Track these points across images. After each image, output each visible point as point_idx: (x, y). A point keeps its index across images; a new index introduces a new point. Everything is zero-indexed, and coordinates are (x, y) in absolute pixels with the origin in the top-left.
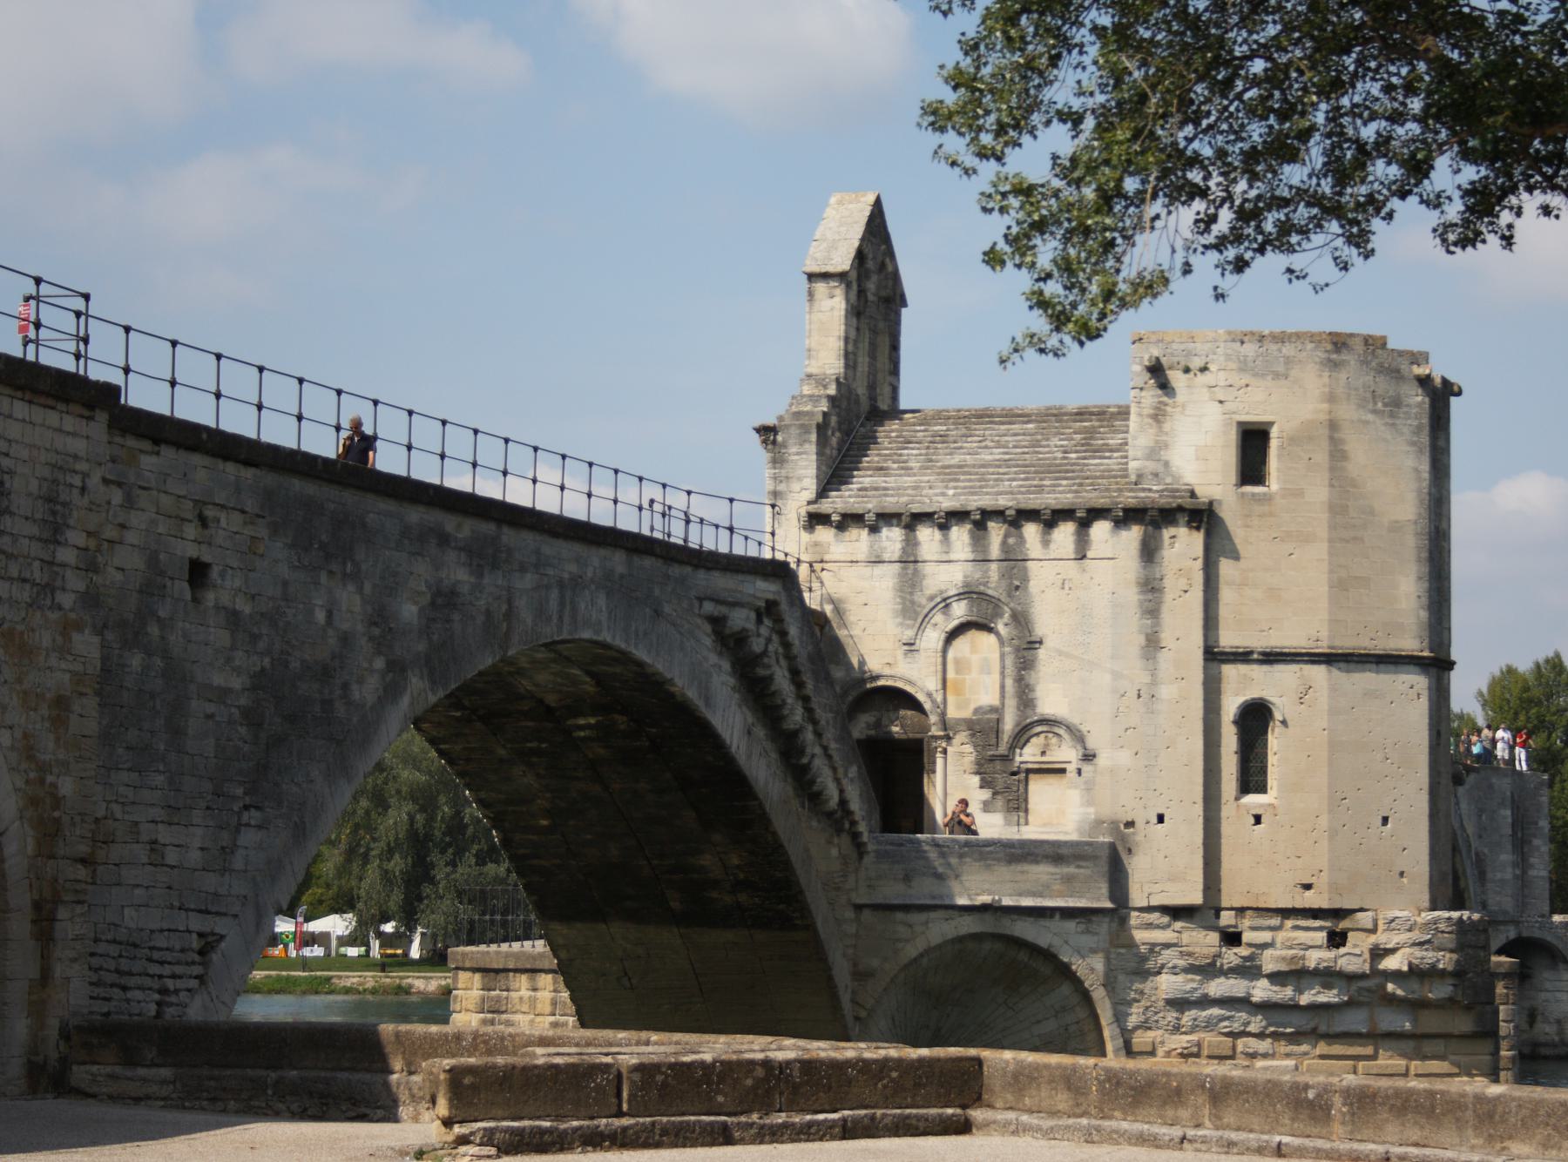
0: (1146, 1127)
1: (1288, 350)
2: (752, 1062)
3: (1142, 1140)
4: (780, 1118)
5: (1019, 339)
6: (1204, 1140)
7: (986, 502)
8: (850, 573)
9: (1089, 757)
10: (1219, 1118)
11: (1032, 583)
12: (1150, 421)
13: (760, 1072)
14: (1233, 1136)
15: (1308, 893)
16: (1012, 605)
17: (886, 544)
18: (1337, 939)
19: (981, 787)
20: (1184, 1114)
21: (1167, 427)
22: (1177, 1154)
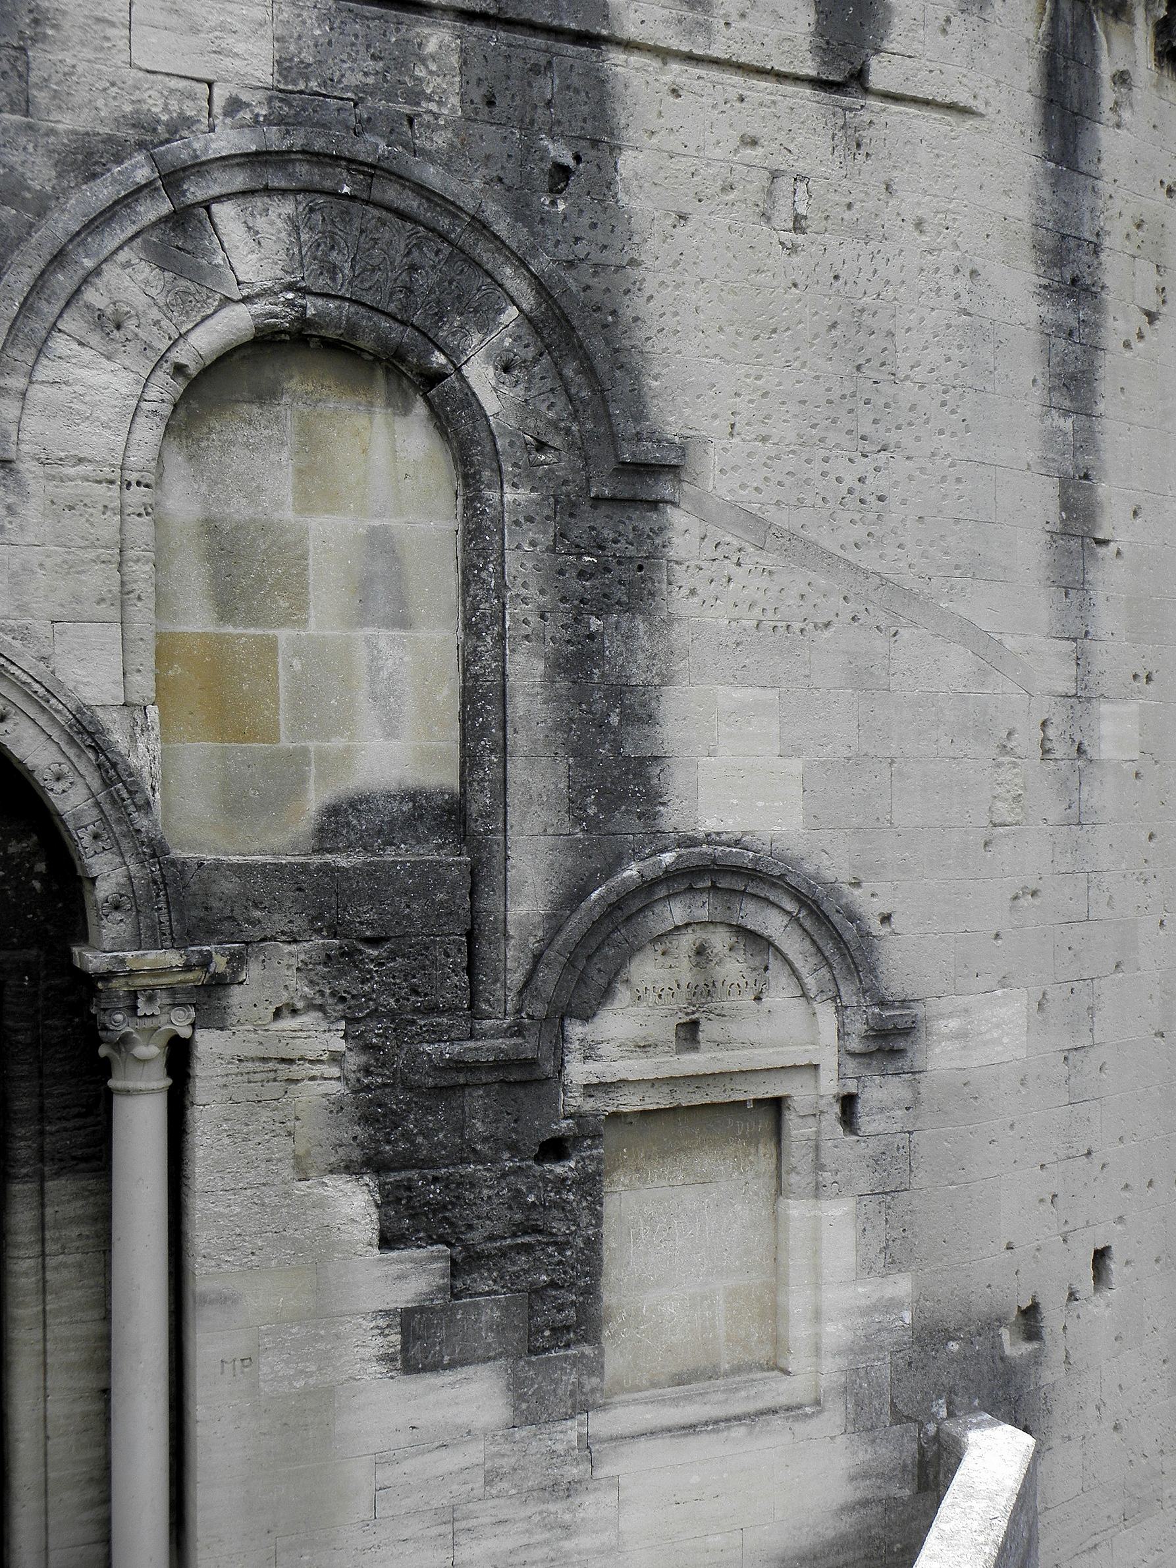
11: (628, 163)
16: (542, 263)
19: (387, 1241)
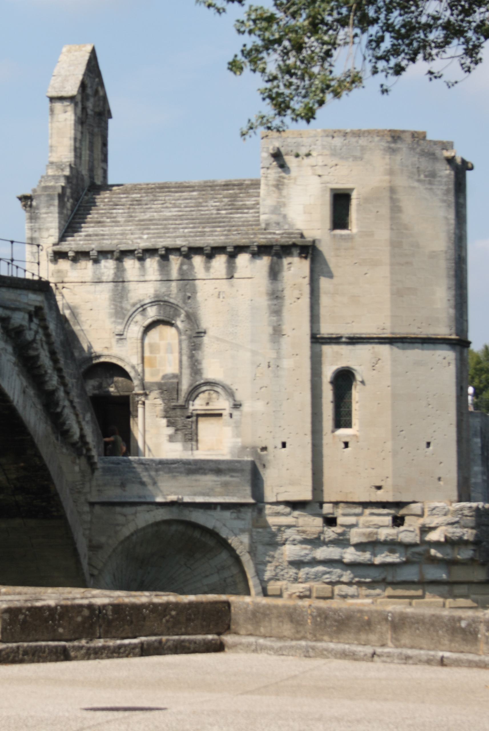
0: (347, 646)
1: (363, 141)
2: (81, 606)
3: (344, 655)
4: (100, 643)
5: (253, 120)
6: (389, 655)
7: (169, 242)
8: (80, 289)
9: (237, 406)
10: (397, 640)
11: (199, 295)
12: (274, 189)
13: (86, 612)
14: (410, 652)
15: (379, 492)
16: (186, 309)
17: (104, 270)
18: (398, 521)
19: (168, 426)
20: (373, 637)
21: (285, 192)
22: (370, 664)
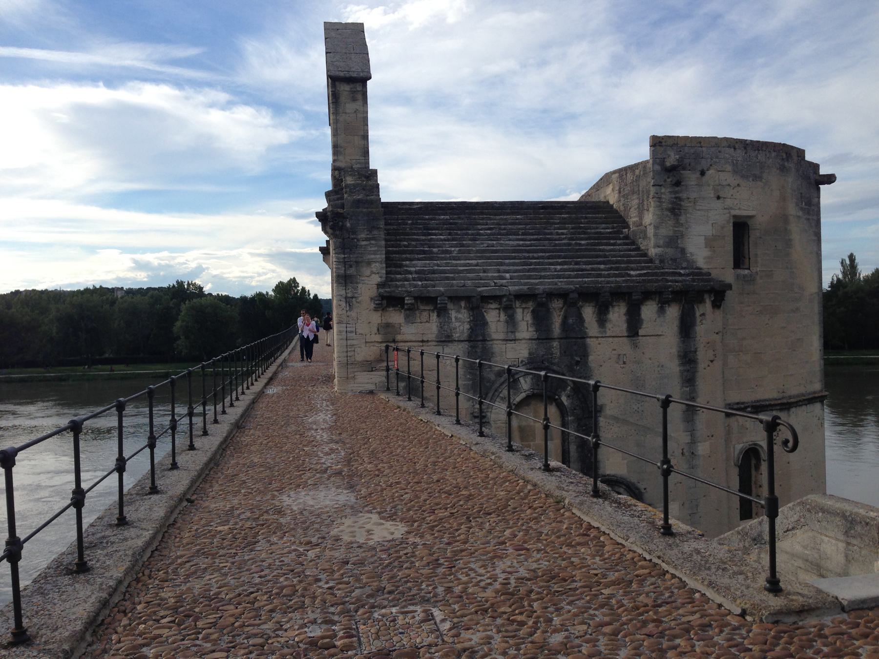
1: (761, 157)
11: (591, 358)
21: (682, 219)
